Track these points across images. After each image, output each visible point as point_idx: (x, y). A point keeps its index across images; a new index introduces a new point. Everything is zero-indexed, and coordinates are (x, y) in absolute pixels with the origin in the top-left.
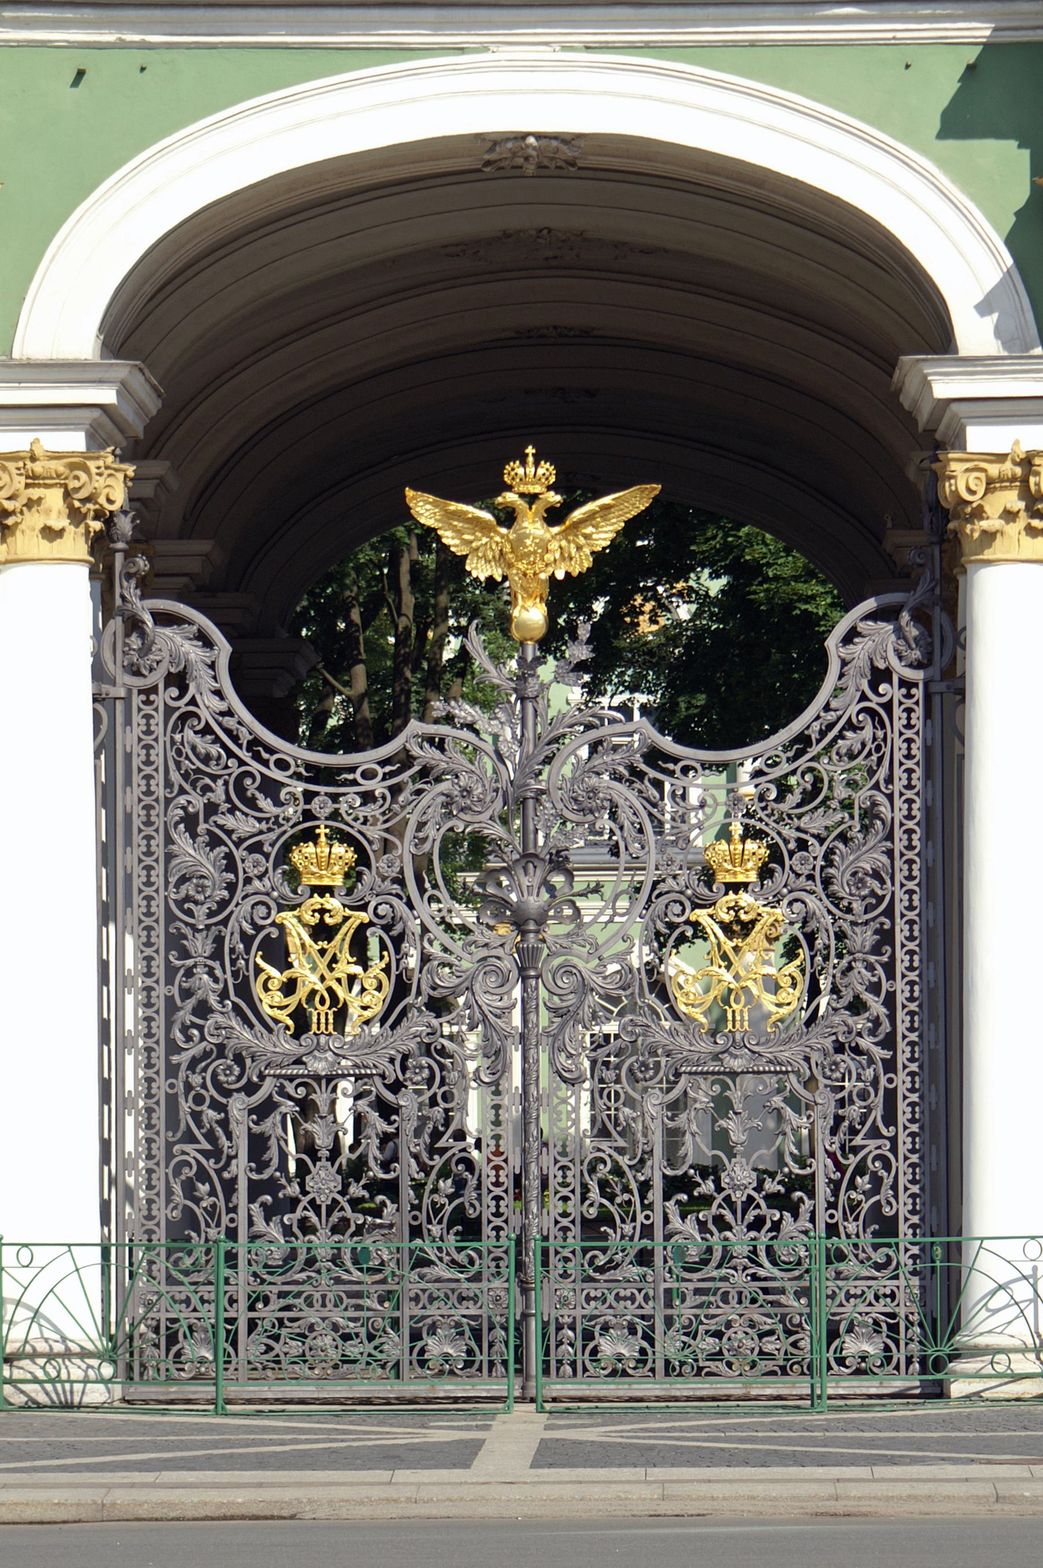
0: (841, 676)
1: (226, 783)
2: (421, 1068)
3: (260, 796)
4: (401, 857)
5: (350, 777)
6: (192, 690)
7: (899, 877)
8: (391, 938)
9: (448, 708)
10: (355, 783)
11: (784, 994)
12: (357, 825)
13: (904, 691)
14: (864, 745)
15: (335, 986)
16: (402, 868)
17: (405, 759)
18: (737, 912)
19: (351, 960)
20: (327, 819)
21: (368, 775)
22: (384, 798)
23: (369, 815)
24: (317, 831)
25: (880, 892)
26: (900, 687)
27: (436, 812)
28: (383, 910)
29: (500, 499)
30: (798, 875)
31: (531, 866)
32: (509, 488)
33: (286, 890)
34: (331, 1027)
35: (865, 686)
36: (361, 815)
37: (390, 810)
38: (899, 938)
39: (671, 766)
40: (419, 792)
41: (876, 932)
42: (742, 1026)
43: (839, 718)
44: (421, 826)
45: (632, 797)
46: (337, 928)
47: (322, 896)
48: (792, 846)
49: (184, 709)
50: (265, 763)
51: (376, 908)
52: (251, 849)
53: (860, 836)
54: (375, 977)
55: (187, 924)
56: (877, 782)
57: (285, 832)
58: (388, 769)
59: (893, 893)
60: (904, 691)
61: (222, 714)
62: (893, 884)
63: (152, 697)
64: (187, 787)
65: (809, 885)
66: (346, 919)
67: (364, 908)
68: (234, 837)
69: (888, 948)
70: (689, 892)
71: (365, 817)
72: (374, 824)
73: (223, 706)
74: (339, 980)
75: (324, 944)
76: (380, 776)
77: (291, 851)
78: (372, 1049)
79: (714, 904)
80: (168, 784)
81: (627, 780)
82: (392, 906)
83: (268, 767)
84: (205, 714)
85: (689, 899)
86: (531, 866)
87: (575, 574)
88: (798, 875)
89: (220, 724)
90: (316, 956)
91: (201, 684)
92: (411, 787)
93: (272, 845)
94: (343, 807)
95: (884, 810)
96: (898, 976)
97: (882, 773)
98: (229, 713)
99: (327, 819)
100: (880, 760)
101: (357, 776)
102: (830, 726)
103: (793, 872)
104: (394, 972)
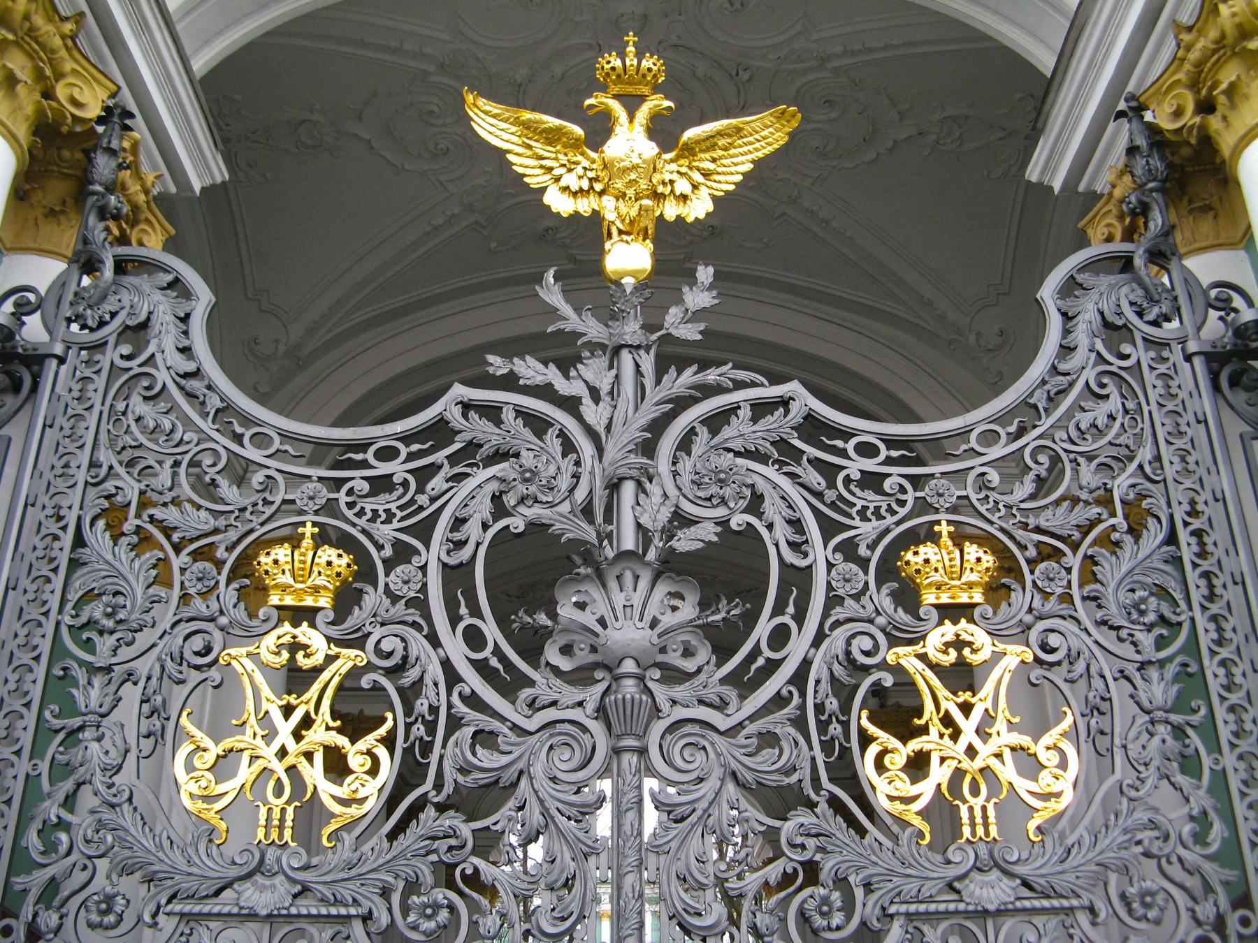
0: (1066, 332)
1: (177, 464)
2: (436, 907)
3: (223, 482)
4: (423, 568)
5: (359, 457)
6: (151, 349)
7: (1196, 597)
8: (400, 691)
9: (510, 366)
10: (364, 464)
11: (1051, 780)
12: (362, 522)
13: (1152, 354)
14: (1111, 417)
15: (303, 765)
16: (425, 585)
17: (440, 432)
18: (959, 650)
19: (332, 724)
20: (316, 513)
21: (387, 454)
22: (405, 484)
23: (381, 509)
24: (300, 530)
25: (1174, 619)
26: (1147, 350)
27: (483, 508)
28: (386, 646)
29: (588, 102)
30: (1046, 595)
31: (628, 576)
32: (604, 88)
33: (240, 614)
34: (288, 833)
35: (1099, 346)
36: (368, 508)
37: (412, 501)
38: (1214, 686)
39: (839, 443)
40: (459, 478)
41: (1176, 678)
42: (987, 834)
43: (1071, 384)
44: (459, 523)
45: (785, 483)
46: (317, 671)
47: (296, 625)
48: (1032, 552)
49: (137, 370)
50: (238, 439)
51: (379, 642)
52: (197, 555)
53: (1128, 539)
54: (369, 753)
55: (81, 663)
56: (1141, 467)
57: (252, 531)
58: (415, 447)
59: (1193, 619)
60: (1152, 354)
61: (186, 376)
62: (1191, 609)
63: (97, 357)
64: (121, 470)
65: (1064, 609)
66: (330, 659)
67: (359, 643)
68: (176, 537)
69: (1200, 702)
70: (881, 620)
71: (375, 512)
72: (388, 521)
73: (191, 367)
74: (309, 756)
75: (292, 699)
76: (403, 456)
77: (257, 555)
78: (353, 872)
79: (924, 638)
80: (93, 464)
81: (776, 461)
82: (403, 640)
83: (242, 445)
84: (163, 376)
85: (883, 630)
86: (628, 576)
87: (690, 219)
88: (1046, 595)
89: (181, 388)
90: (277, 716)
91: (164, 341)
92: (447, 471)
93: (230, 549)
94: (343, 498)
95: (1156, 502)
96: (1225, 746)
97: (1145, 454)
98: (196, 374)
99: (316, 513)
100: (1139, 437)
101: (370, 456)
102: (1062, 392)
103: (1040, 590)
104: (400, 744)
